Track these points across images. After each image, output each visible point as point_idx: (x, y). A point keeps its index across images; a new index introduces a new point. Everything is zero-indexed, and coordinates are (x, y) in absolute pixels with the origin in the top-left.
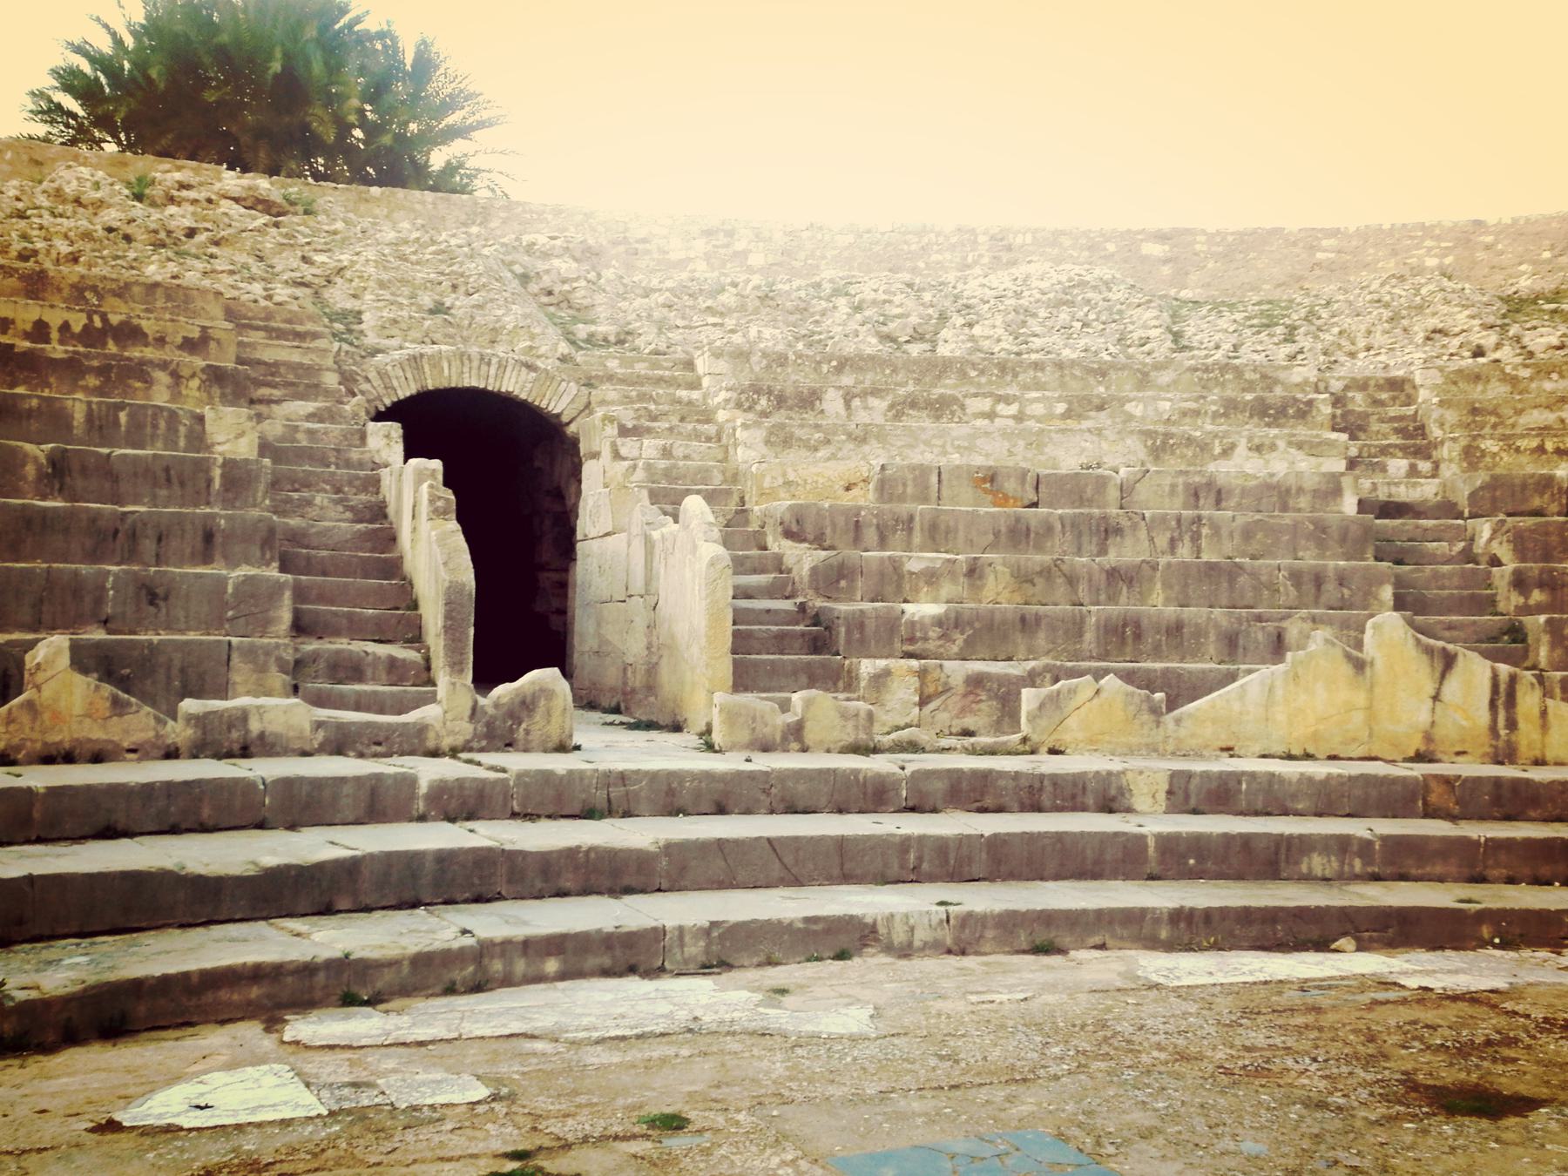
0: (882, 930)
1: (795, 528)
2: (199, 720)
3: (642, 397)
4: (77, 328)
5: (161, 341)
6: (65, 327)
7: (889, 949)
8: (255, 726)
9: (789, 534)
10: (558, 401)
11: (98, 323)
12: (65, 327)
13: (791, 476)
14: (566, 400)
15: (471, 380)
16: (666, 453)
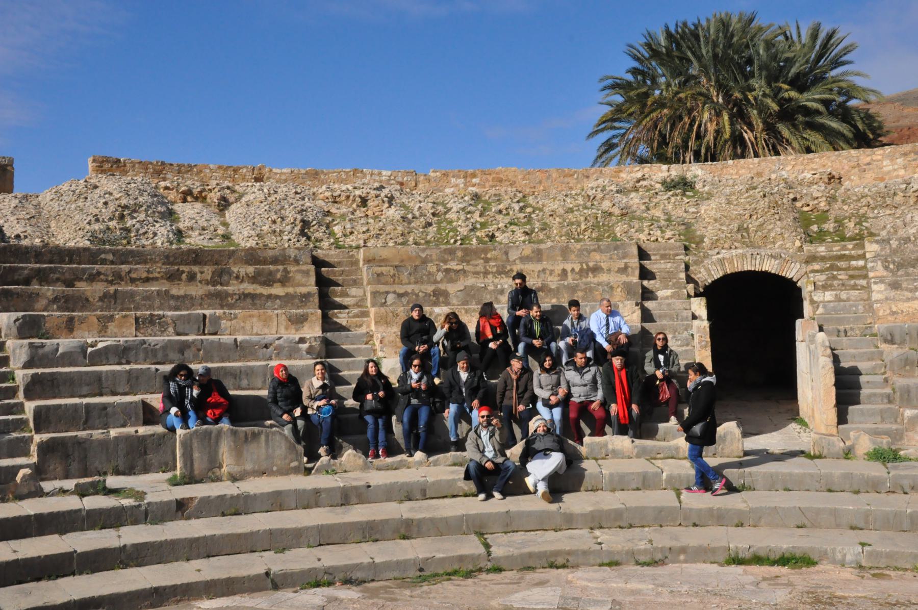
0: (830, 554)
1: (889, 338)
3: (832, 268)
4: (577, 270)
5: (609, 270)
6: (573, 270)
7: (834, 562)
8: (610, 447)
9: (886, 341)
10: (791, 272)
11: (585, 266)
12: (573, 270)
13: (894, 309)
14: (794, 271)
15: (748, 267)
16: (838, 299)
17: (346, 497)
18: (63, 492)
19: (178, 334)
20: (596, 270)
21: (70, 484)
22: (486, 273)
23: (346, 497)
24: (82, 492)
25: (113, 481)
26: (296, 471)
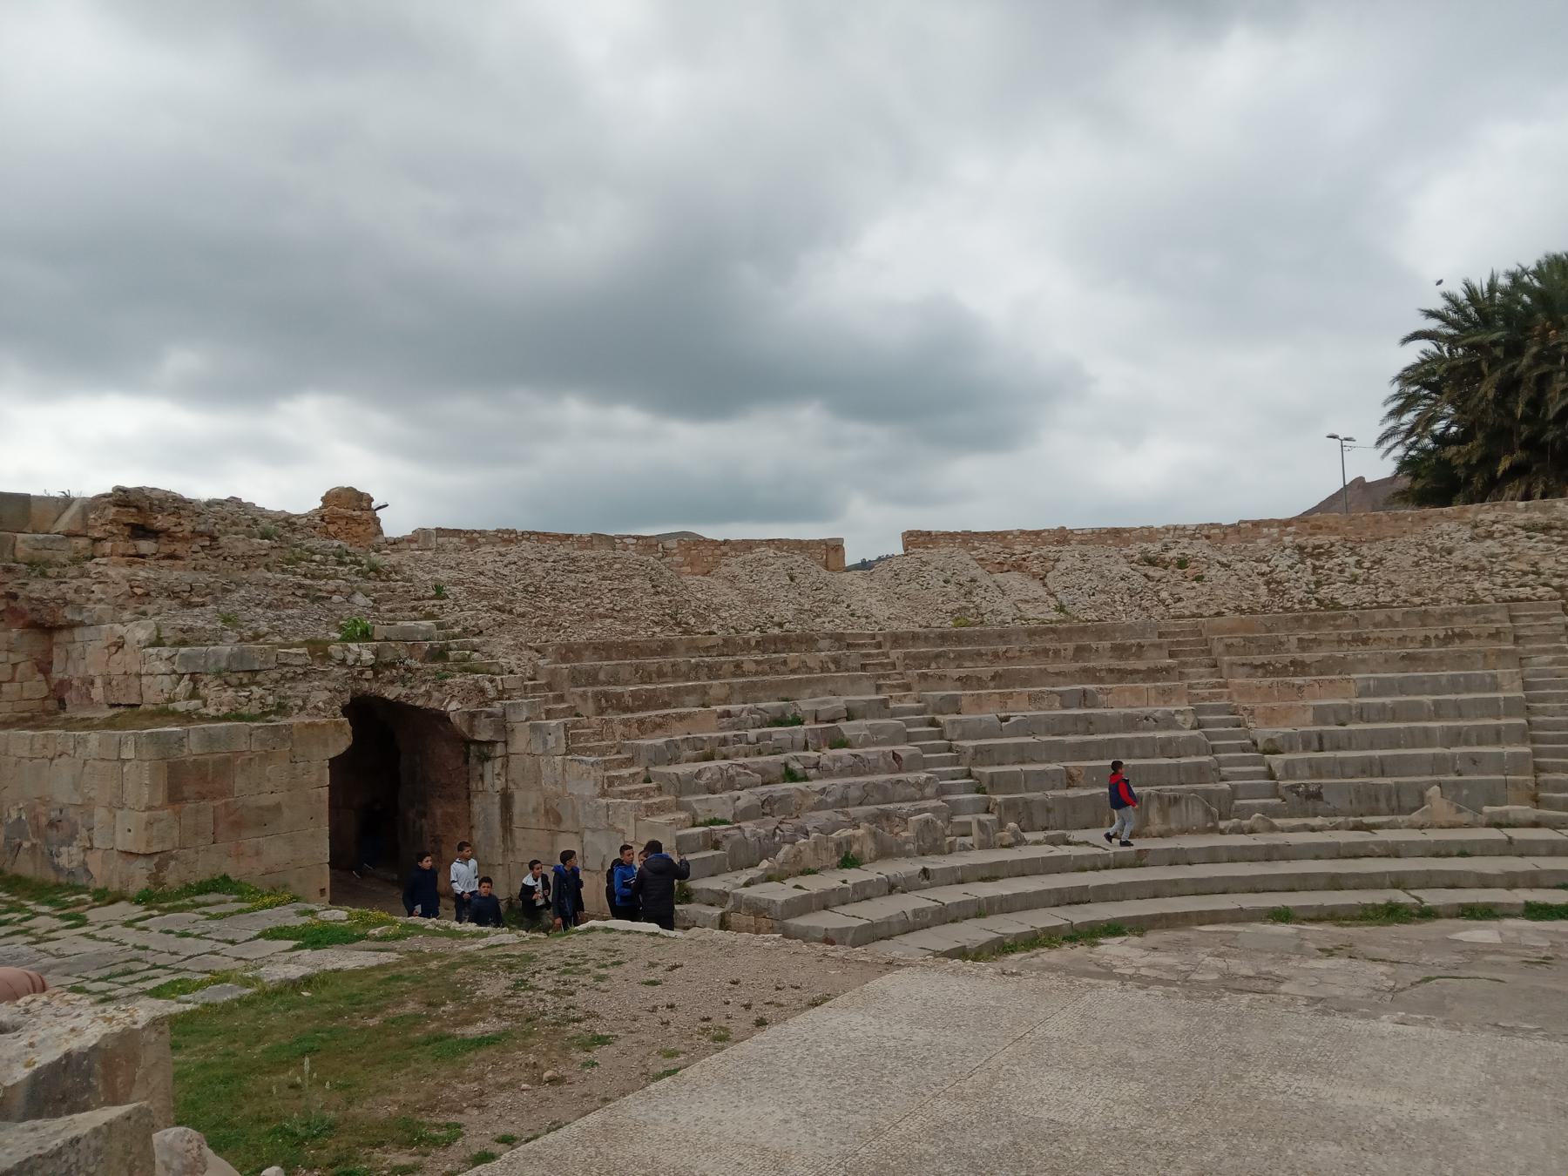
2: (1491, 814)
17: (1270, 854)
18: (1037, 843)
19: (1064, 707)
20: (1464, 636)
21: (1040, 836)
22: (1340, 641)
23: (1270, 854)
24: (1052, 842)
25: (1076, 835)
26: (1214, 830)
